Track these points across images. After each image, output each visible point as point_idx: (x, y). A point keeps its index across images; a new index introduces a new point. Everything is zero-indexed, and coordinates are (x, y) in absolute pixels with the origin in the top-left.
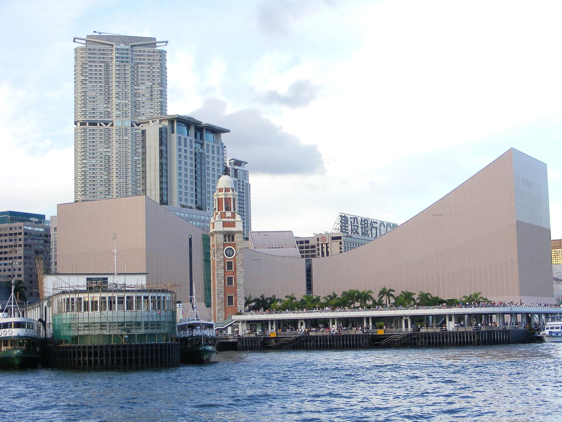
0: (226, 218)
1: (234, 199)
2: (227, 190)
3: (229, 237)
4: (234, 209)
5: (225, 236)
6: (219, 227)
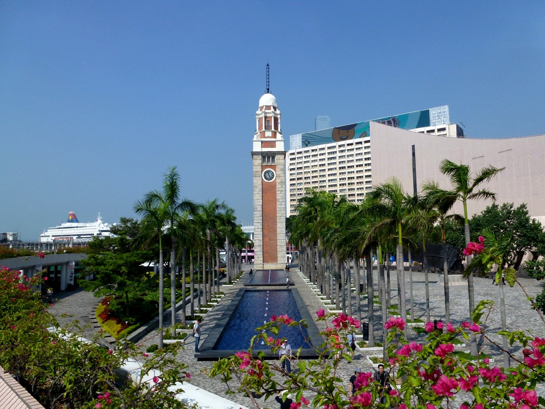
0: (265, 137)
1: (276, 119)
2: (268, 107)
3: (269, 158)
4: (276, 127)
5: (264, 158)
6: (257, 147)
